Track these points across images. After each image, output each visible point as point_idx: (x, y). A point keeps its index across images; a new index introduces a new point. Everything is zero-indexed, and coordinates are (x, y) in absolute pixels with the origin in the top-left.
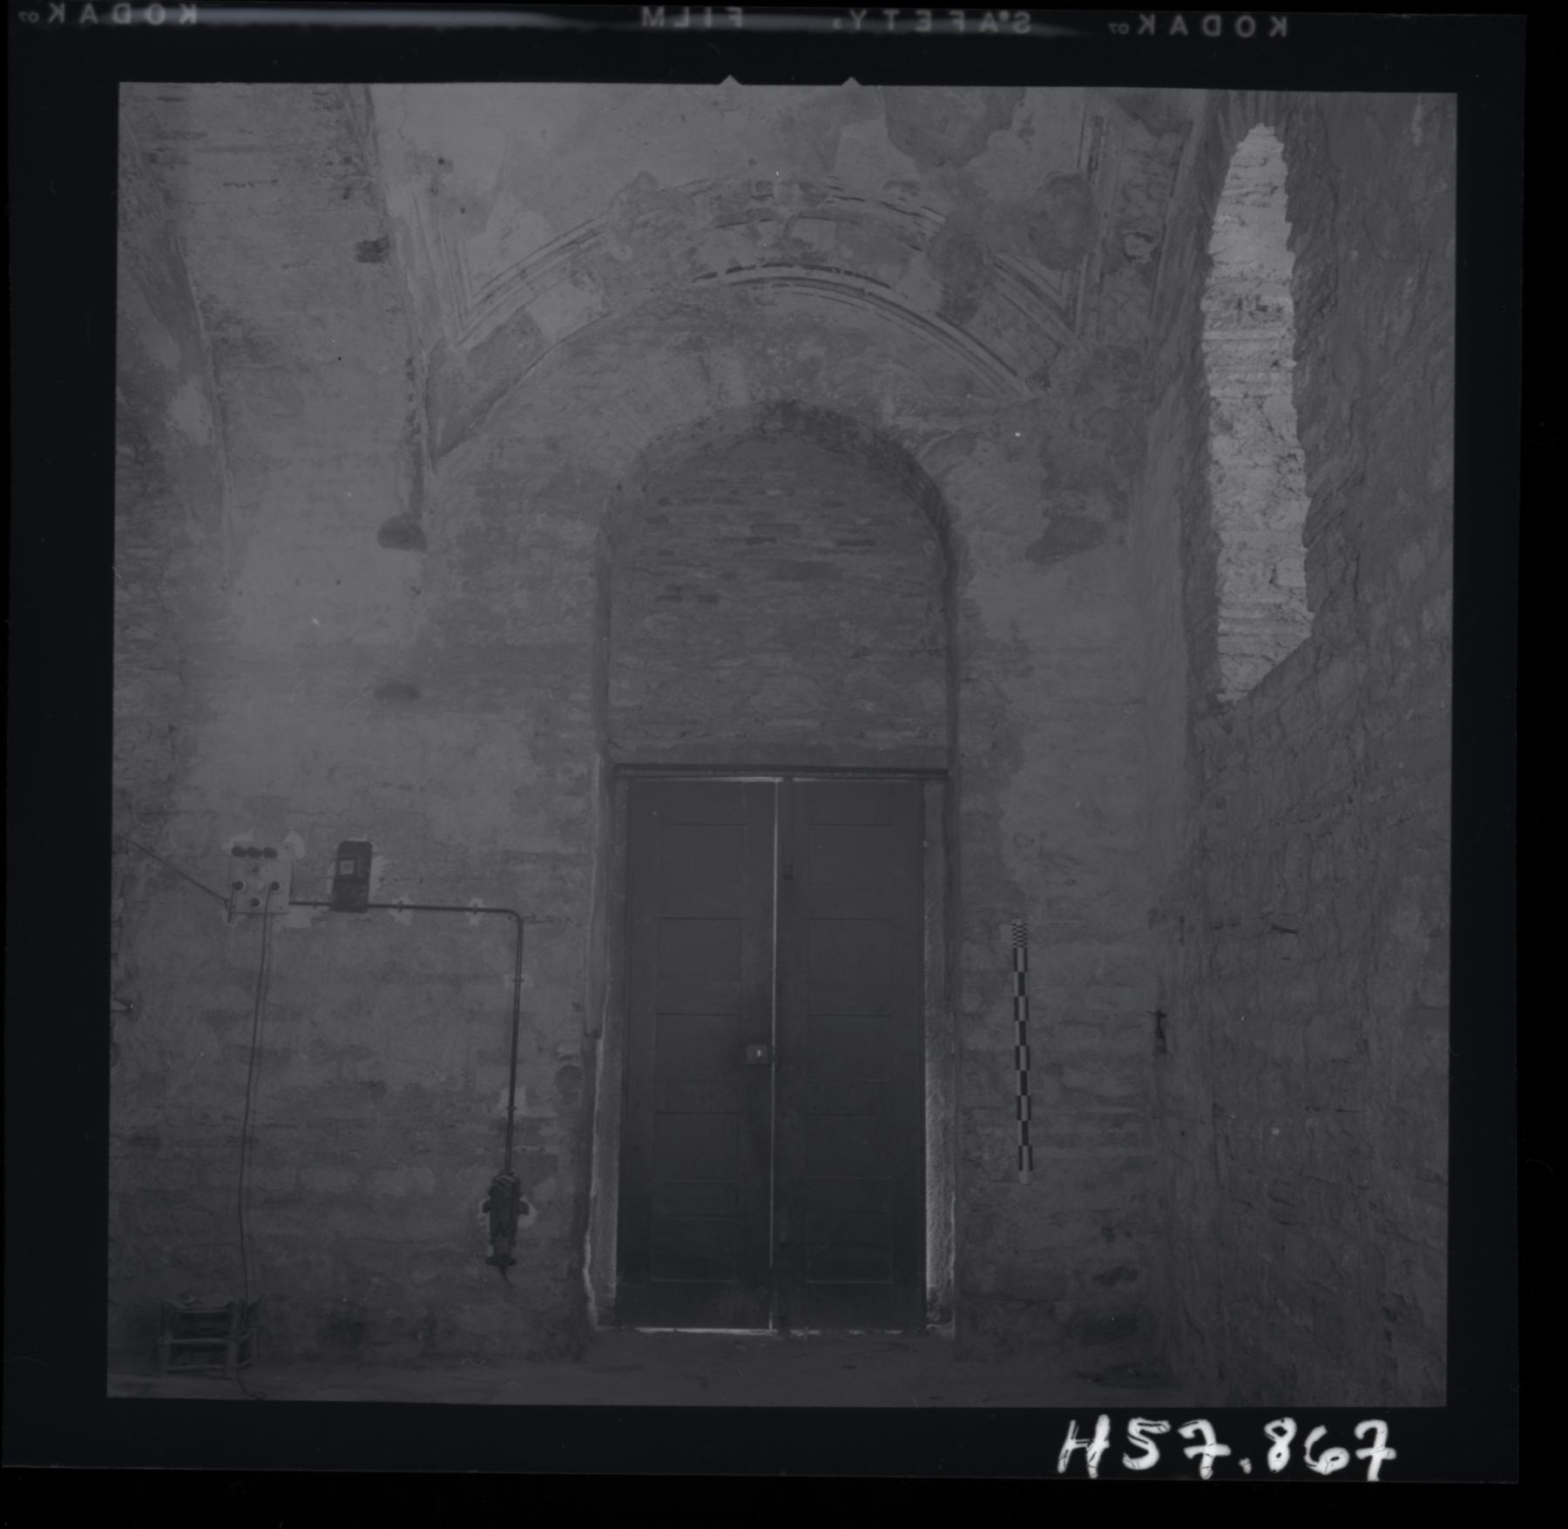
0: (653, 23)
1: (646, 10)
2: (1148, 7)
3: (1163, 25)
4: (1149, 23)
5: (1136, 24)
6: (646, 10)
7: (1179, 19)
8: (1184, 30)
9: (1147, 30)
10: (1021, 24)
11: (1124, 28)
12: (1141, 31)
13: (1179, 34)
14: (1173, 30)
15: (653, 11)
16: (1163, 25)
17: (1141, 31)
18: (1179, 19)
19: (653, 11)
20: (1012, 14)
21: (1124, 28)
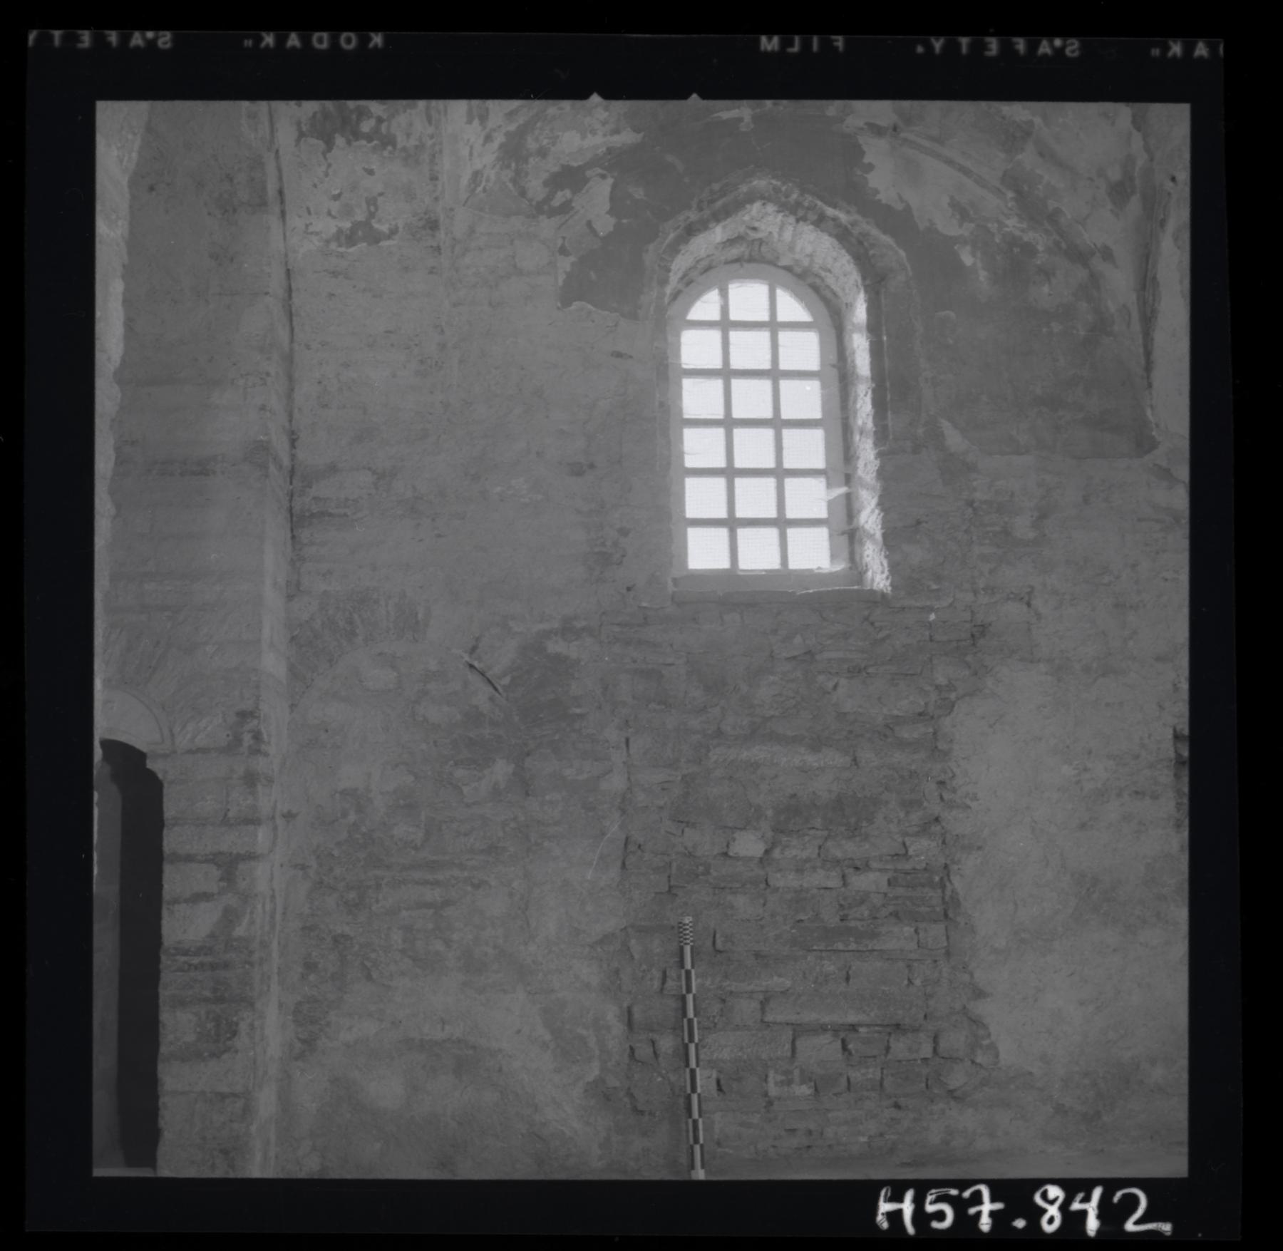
0: (769, 48)
1: (764, 39)
2: (1176, 35)
3: (1188, 49)
4: (1176, 49)
5: (1166, 48)
6: (764, 39)
10: (1073, 48)
11: (1156, 52)
15: (770, 40)
16: (1188, 49)
17: (1170, 54)
19: (770, 40)
20: (1065, 41)
21: (1156, 52)
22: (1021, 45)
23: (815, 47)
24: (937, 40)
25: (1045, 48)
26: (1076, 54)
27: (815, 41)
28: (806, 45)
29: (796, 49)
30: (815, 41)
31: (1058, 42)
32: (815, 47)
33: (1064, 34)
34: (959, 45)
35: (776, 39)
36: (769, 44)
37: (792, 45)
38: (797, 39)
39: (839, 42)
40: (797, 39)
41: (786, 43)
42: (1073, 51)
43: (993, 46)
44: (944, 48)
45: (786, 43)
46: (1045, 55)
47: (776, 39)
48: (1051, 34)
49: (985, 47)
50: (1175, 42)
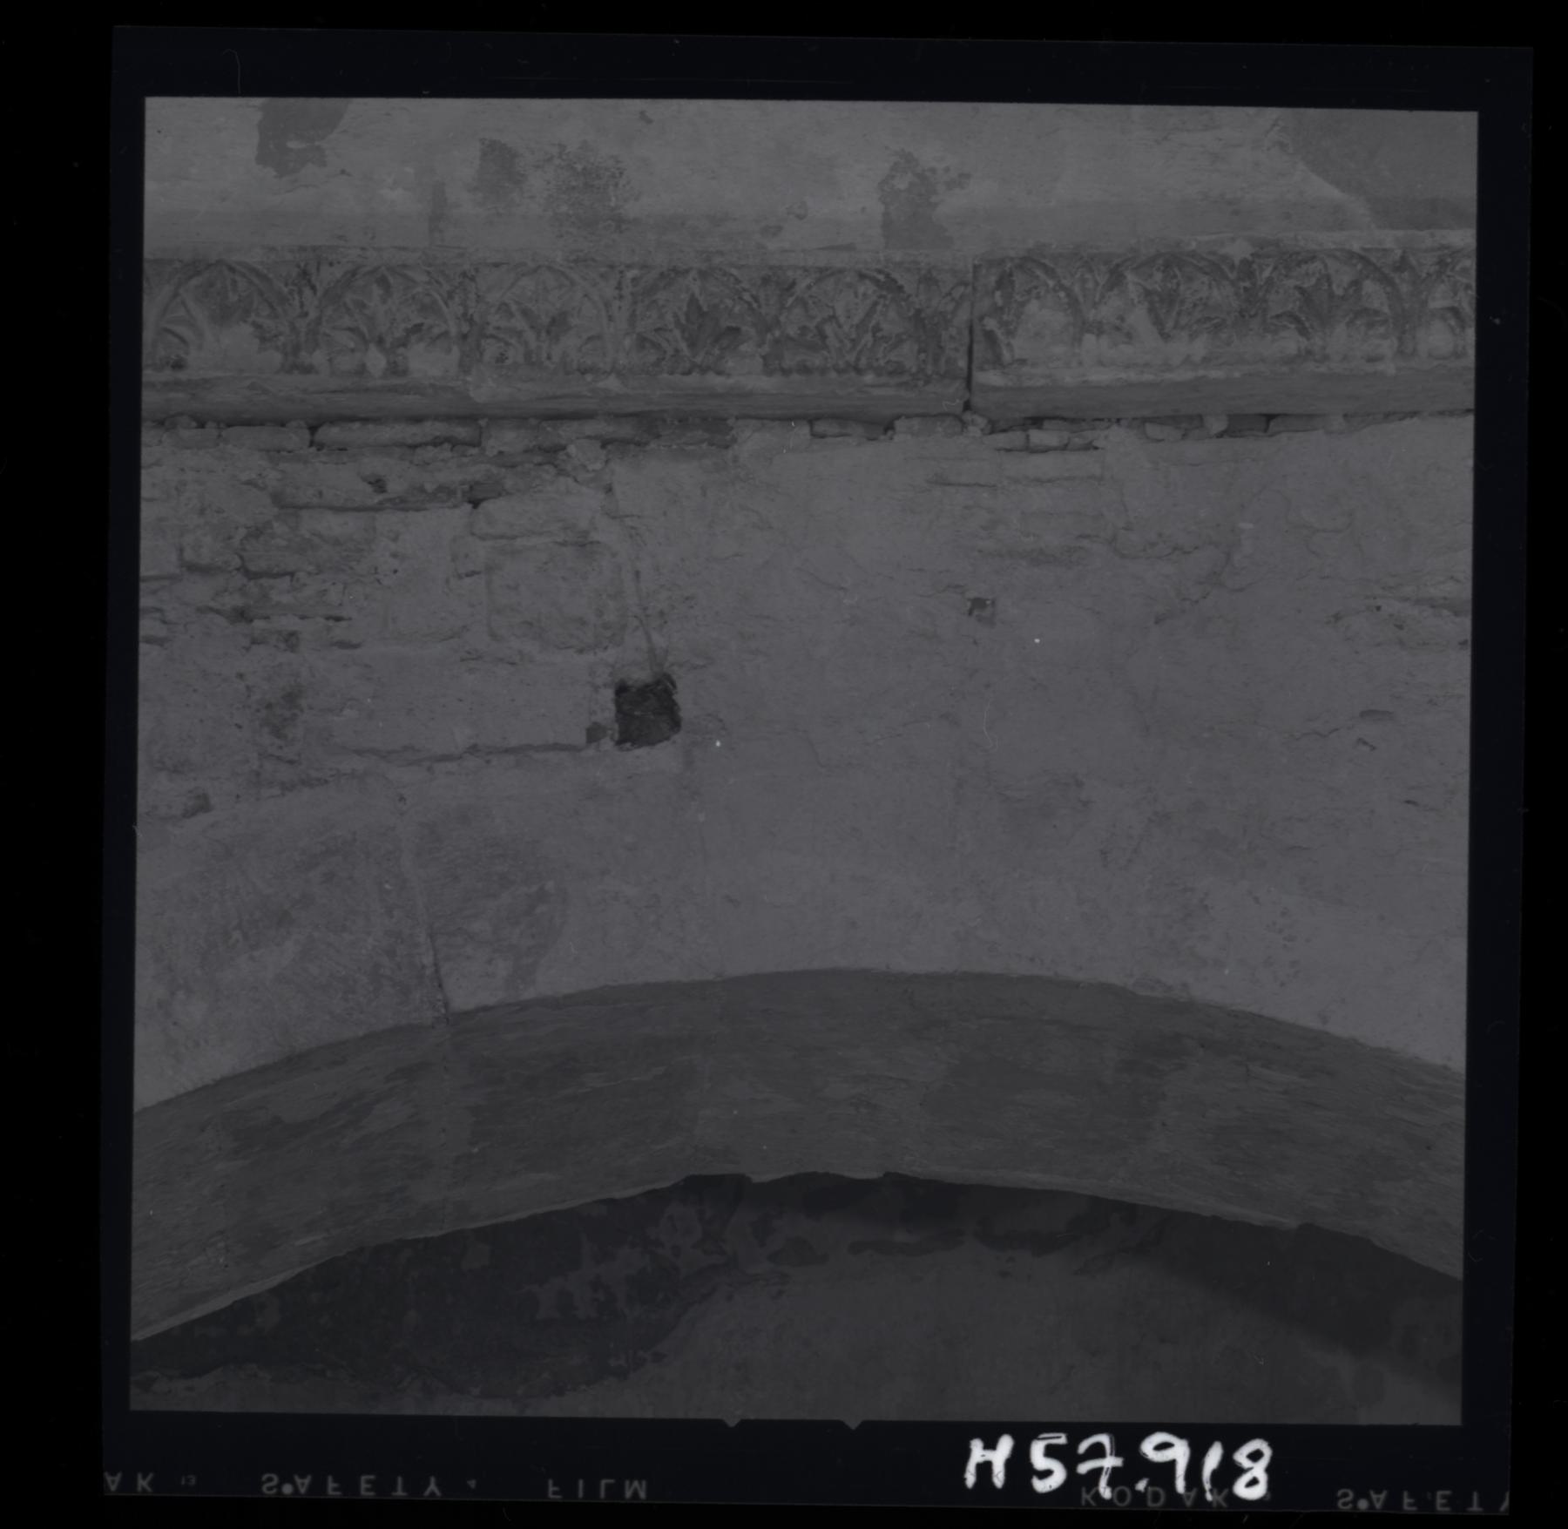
0: (636, 1483)
1: (642, 1495)
3: (128, 1482)
6: (642, 1495)
7: (113, 1488)
8: (109, 1479)
9: (144, 1477)
10: (270, 1485)
12: (150, 1476)
13: (113, 1474)
14: (118, 1478)
15: (635, 1494)
16: (128, 1482)
17: (150, 1476)
18: (113, 1488)
19: (635, 1494)
20: (280, 1492)
22: (332, 1488)
23: (581, 1483)
24: (433, 1494)
25: (303, 1484)
26: (265, 1477)
27: (581, 1494)
28: (592, 1488)
29: (604, 1482)
30: (581, 1494)
31: (287, 1489)
32: (581, 1483)
33: (280, 1502)
34: (405, 1489)
35: (628, 1494)
36: (636, 1489)
37: (608, 1487)
38: (603, 1494)
39: (552, 1492)
40: (603, 1494)
41: (616, 1490)
42: (270, 1480)
43: (365, 1489)
44: (428, 1484)
45: (616, 1490)
46: (303, 1476)
47: (628, 1494)
48: (294, 1502)
49: (375, 1485)
50: (144, 1490)
